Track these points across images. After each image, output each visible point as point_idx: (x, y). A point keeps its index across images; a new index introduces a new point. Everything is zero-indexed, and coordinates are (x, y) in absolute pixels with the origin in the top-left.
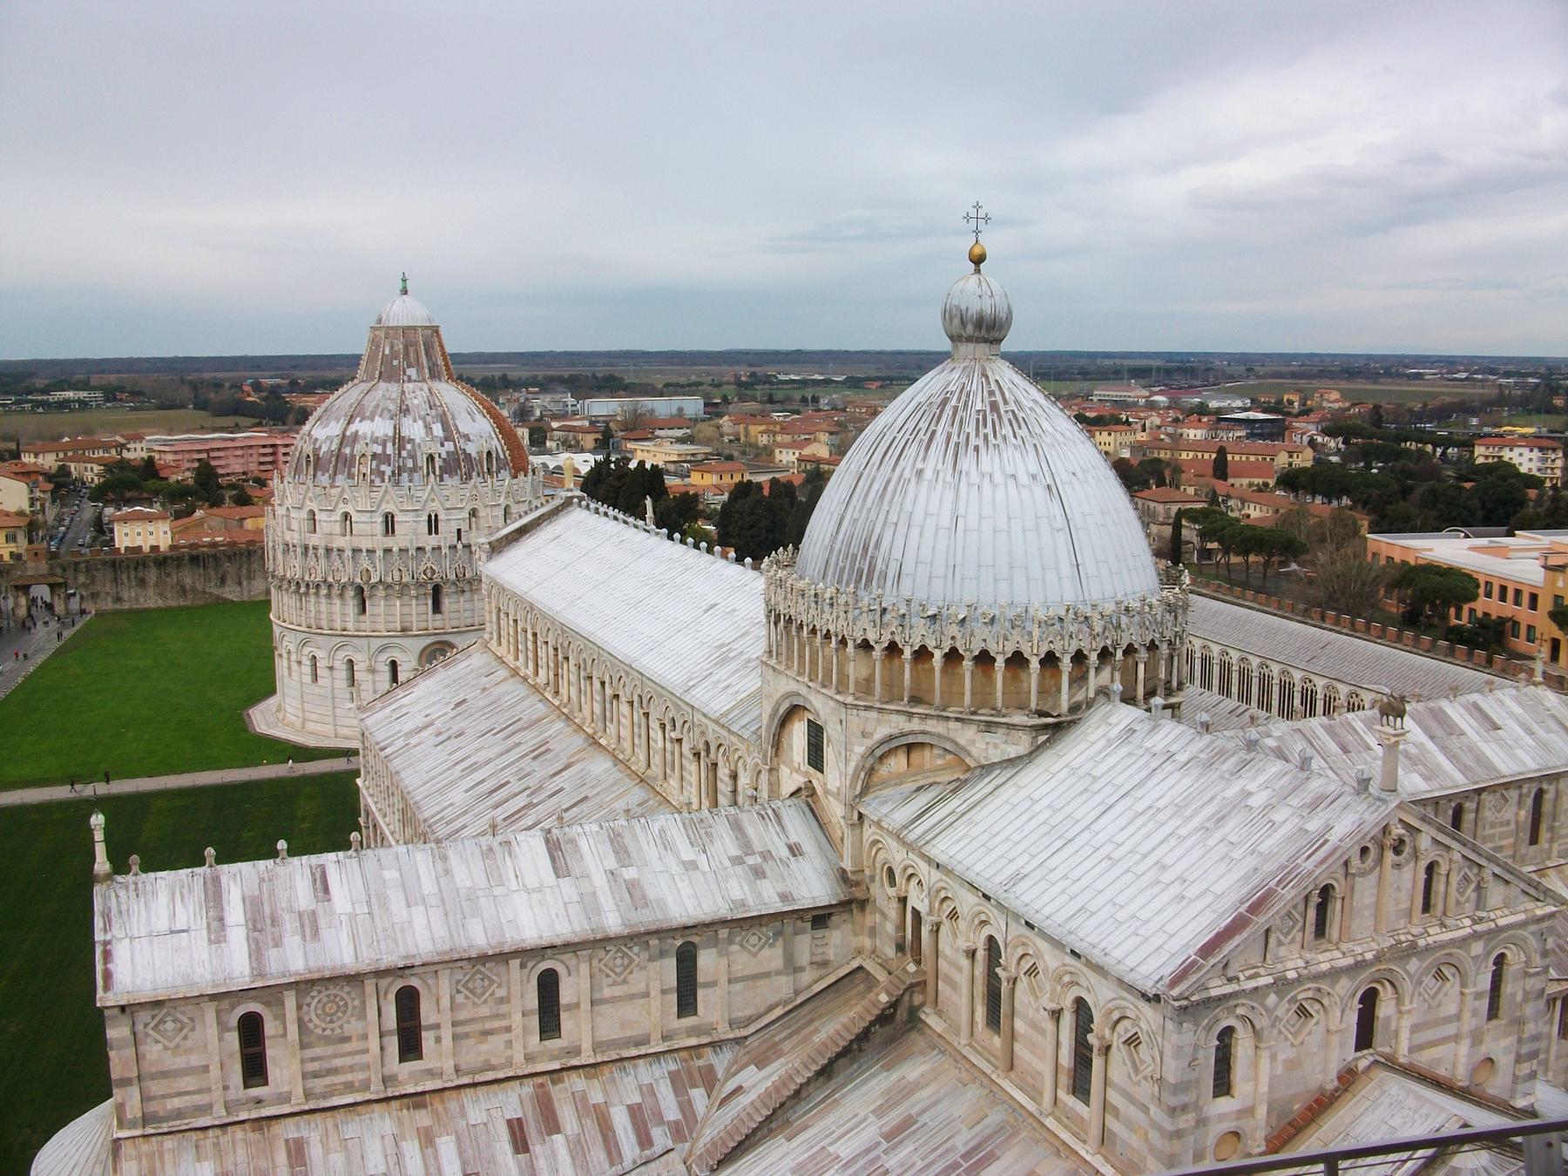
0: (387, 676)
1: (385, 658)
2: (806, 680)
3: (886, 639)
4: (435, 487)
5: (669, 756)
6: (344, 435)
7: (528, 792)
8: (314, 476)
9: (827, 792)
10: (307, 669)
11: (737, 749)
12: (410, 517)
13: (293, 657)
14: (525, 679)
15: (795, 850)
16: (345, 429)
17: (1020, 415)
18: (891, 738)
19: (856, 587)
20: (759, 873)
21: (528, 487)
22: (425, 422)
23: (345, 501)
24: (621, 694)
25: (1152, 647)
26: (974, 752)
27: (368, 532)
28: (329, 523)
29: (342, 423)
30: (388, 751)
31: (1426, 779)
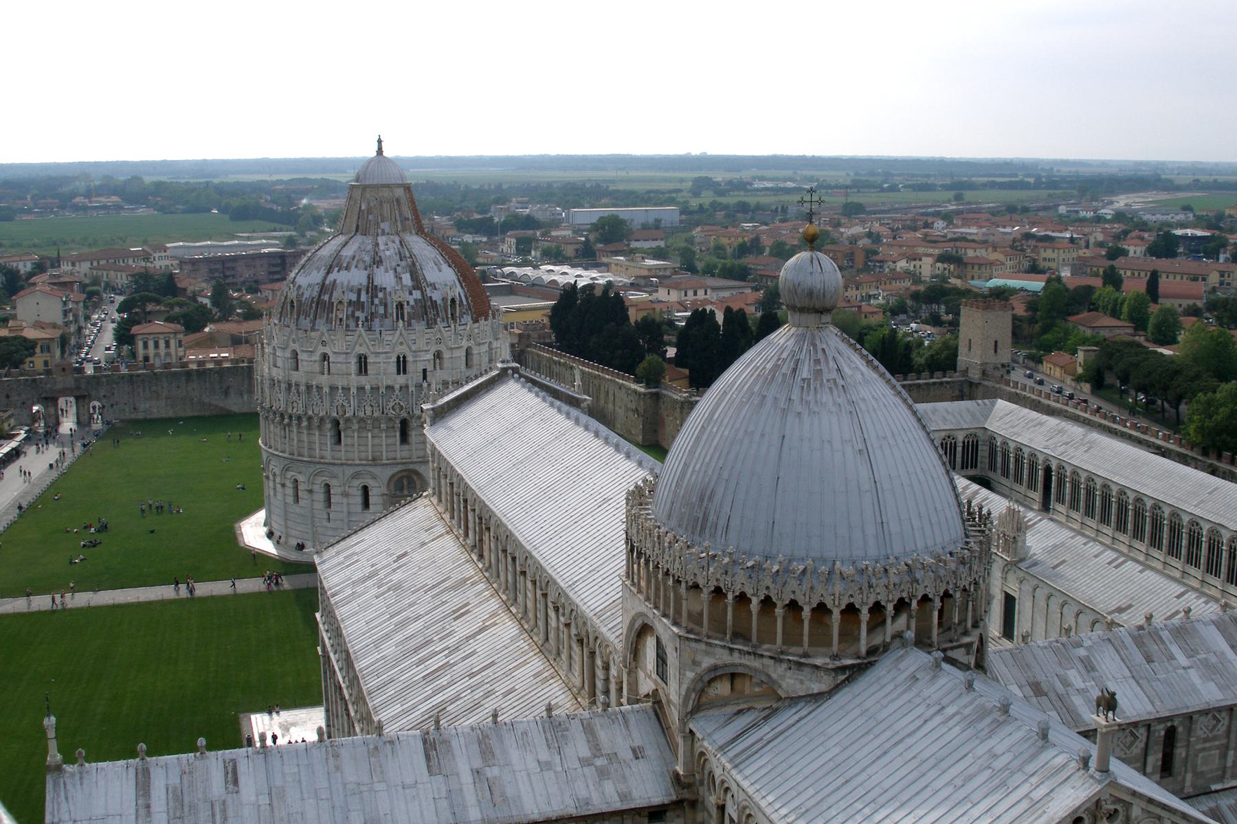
0: (359, 500)
1: (358, 483)
3: (713, 584)
4: (404, 332)
6: (324, 284)
7: (447, 652)
8: (297, 319)
9: (669, 701)
10: (290, 491)
12: (381, 359)
13: (278, 480)
15: (637, 753)
16: (325, 278)
17: (841, 382)
18: (715, 668)
20: (603, 774)
21: (488, 329)
22: (396, 271)
23: (324, 343)
24: (528, 572)
25: (946, 595)
26: (784, 685)
27: (345, 373)
28: (309, 363)
29: (323, 272)
30: (337, 598)
31: (1221, 688)
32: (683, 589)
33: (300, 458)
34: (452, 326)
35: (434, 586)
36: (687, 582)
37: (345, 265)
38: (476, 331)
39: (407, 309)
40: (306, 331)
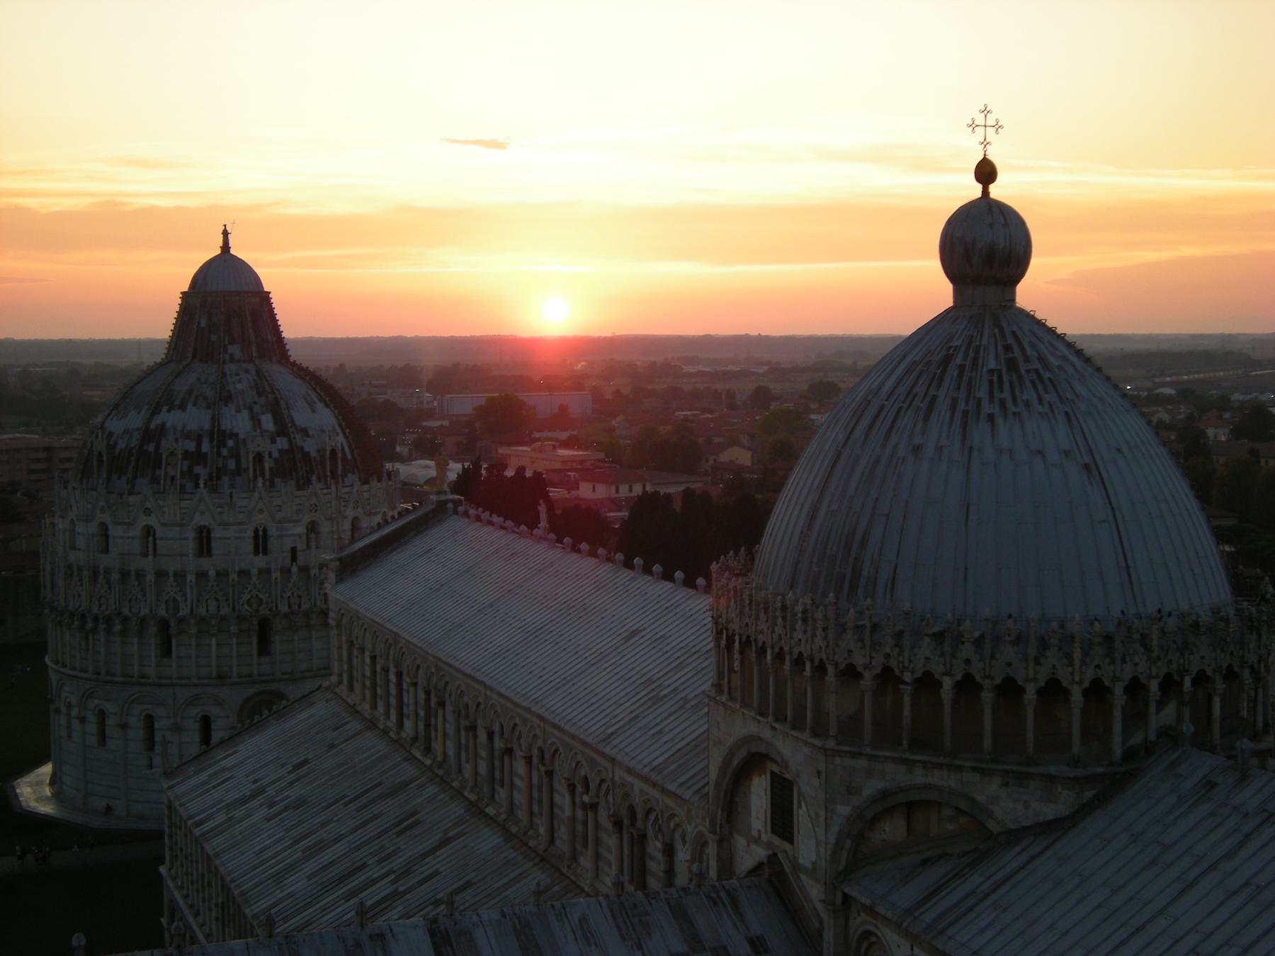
2: (770, 719)
3: (879, 661)
5: (579, 827)
7: (393, 877)
9: (797, 868)
10: (92, 728)
11: (673, 816)
13: (75, 712)
14: (385, 732)
16: (150, 421)
17: (1046, 375)
18: (884, 795)
19: (837, 598)
23: (148, 512)
24: (516, 747)
25: (1230, 675)
30: (206, 827)
32: (831, 677)
33: (109, 678)
34: (333, 488)
35: (357, 797)
36: (836, 665)
37: (178, 402)
38: (366, 495)
39: (268, 464)
40: (121, 495)
